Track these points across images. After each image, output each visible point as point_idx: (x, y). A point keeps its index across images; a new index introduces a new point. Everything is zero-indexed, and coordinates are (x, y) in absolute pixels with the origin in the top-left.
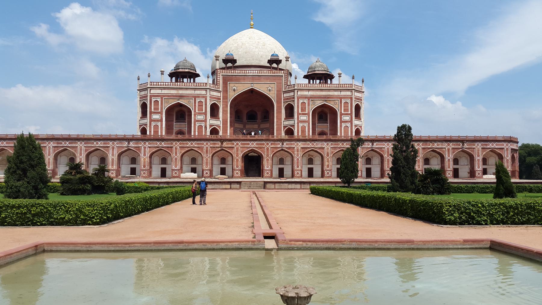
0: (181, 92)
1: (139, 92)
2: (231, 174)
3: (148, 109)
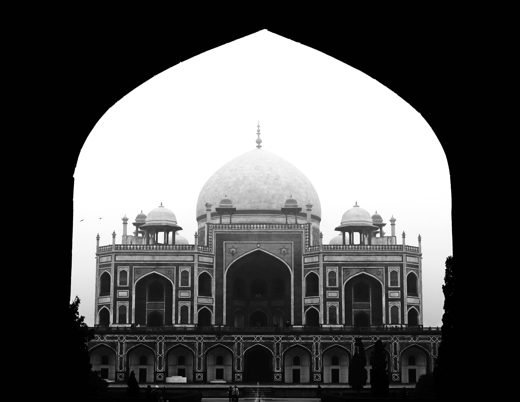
0: (157, 258)
1: (98, 257)
2: (230, 378)
3: (112, 284)
